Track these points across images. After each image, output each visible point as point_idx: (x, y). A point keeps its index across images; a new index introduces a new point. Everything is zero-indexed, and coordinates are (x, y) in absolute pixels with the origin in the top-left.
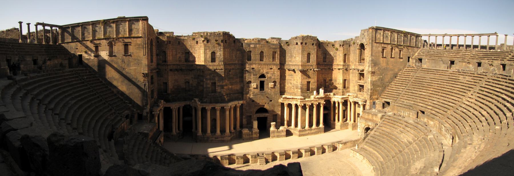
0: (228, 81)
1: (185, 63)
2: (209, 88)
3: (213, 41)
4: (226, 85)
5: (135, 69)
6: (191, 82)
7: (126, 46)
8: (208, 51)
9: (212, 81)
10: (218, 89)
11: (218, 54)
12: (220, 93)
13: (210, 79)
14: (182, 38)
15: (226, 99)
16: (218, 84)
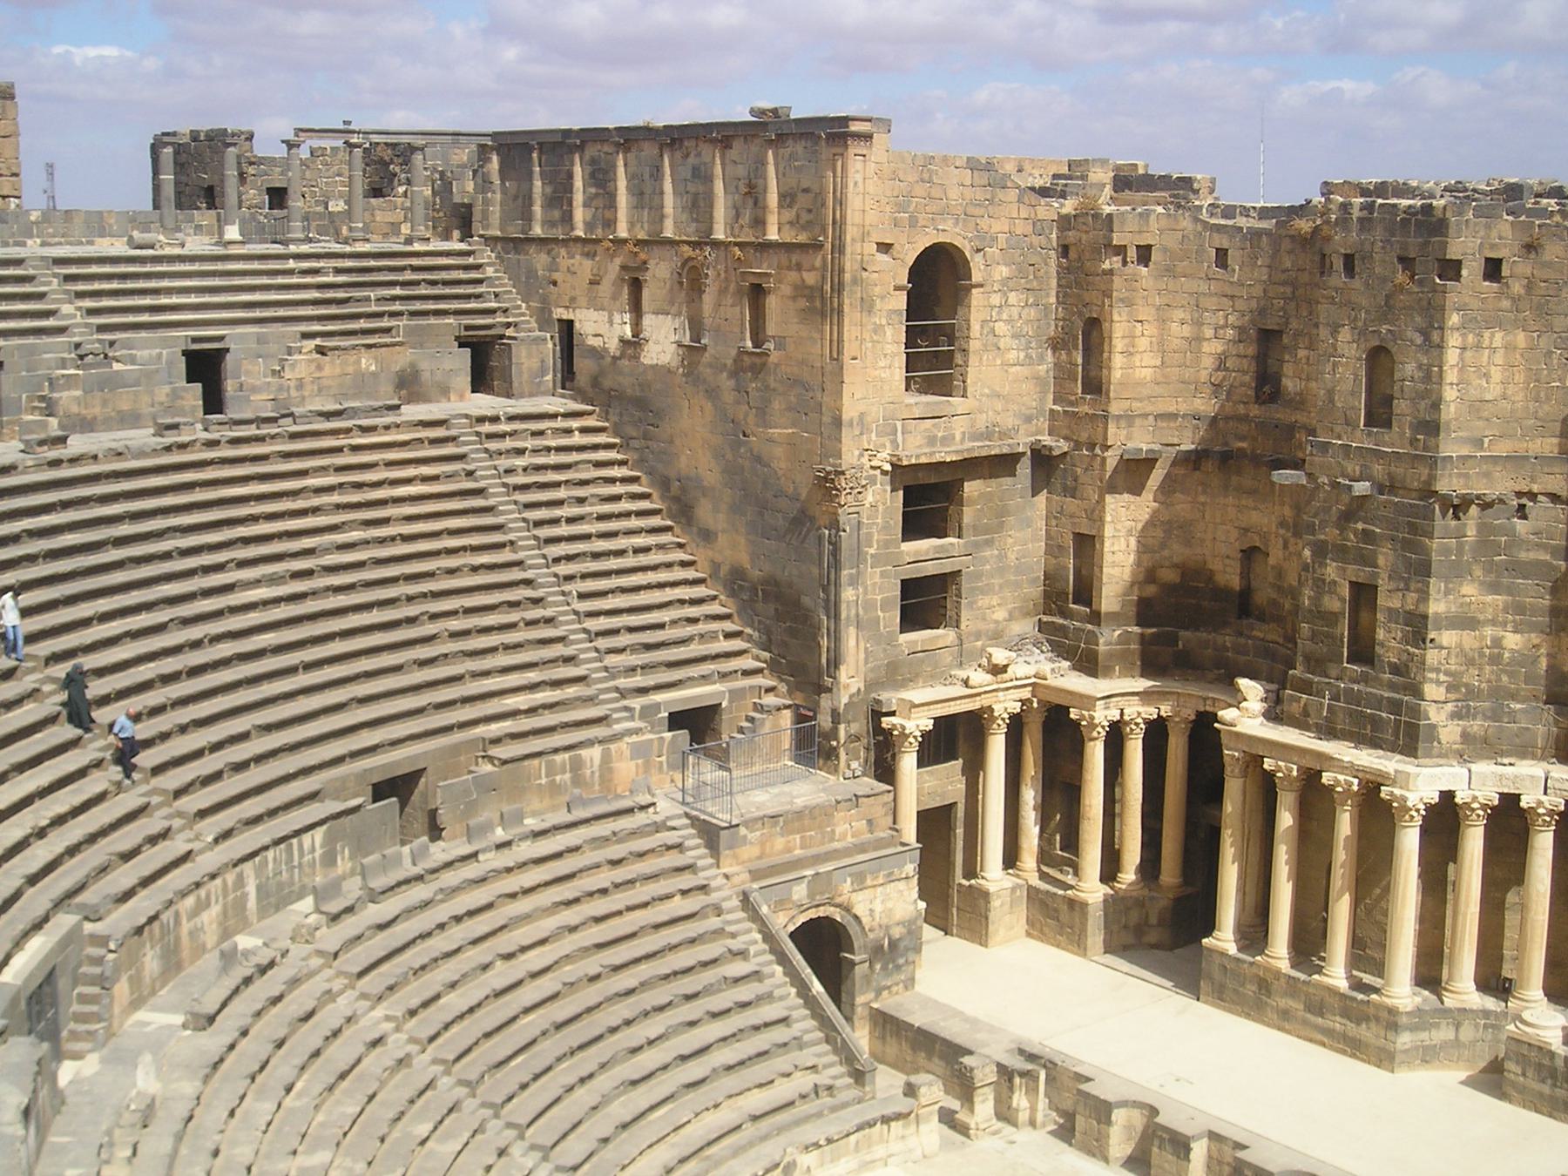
0: (1494, 588)
1: (1255, 411)
2: (1332, 618)
3: (1383, 263)
4: (1466, 622)
5: (791, 443)
6: (1276, 555)
7: (757, 293)
8: (1345, 334)
9: (1357, 573)
10: (1389, 640)
11: (1410, 368)
12: (1396, 670)
13: (1342, 553)
14: (1242, 222)
15: (1450, 733)
16: (1388, 600)
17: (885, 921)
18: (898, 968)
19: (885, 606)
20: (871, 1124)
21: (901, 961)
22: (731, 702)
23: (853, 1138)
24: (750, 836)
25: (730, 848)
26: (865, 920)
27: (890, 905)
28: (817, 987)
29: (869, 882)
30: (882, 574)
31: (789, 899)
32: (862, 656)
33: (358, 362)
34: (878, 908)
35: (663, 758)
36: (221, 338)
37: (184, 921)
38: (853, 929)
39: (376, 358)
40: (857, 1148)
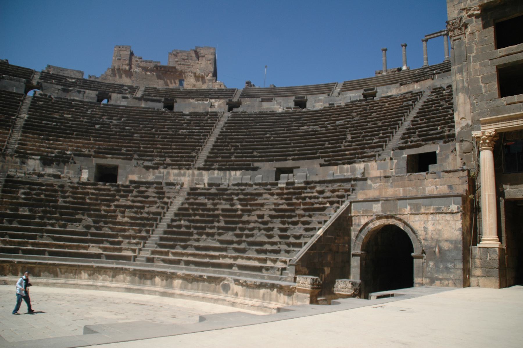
17: (436, 237)
18: (447, 269)
19: (485, 80)
20: (272, 287)
21: (450, 265)
22: (441, 151)
23: (262, 291)
24: (373, 185)
25: (363, 189)
26: (421, 233)
27: (440, 227)
28: (320, 232)
29: (423, 211)
30: (481, 65)
31: (371, 211)
32: (468, 107)
33: (414, 86)
34: (430, 227)
35: (393, 170)
36: (373, 89)
37: (172, 175)
38: (411, 236)
39: (420, 85)
40: (263, 298)
